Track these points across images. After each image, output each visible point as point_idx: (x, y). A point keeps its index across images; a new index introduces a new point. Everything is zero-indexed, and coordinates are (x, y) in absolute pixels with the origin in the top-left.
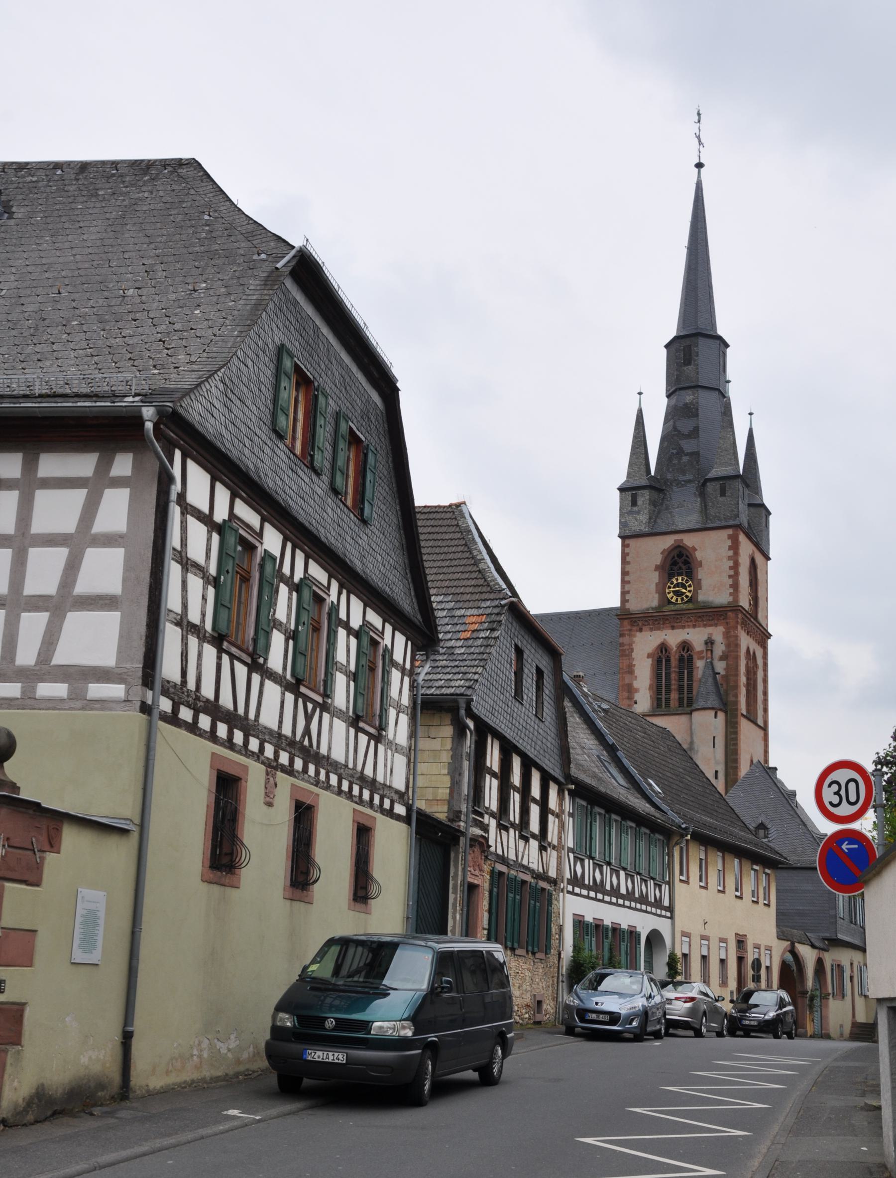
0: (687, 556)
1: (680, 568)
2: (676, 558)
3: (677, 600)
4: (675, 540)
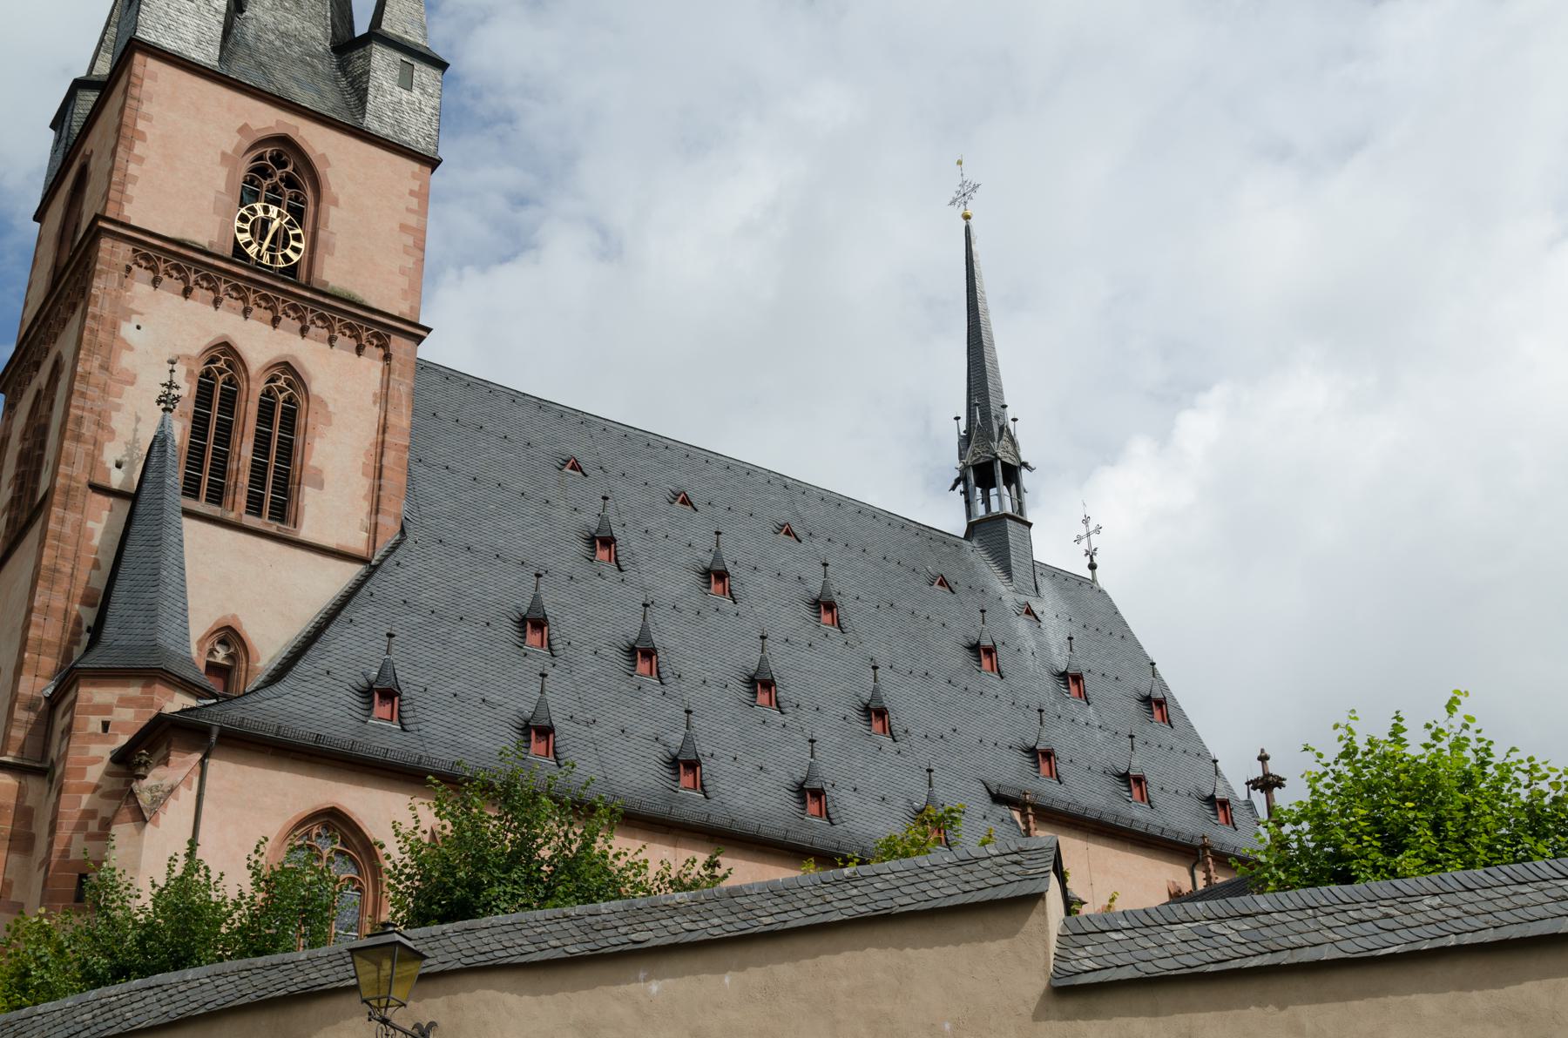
4: (277, 121)
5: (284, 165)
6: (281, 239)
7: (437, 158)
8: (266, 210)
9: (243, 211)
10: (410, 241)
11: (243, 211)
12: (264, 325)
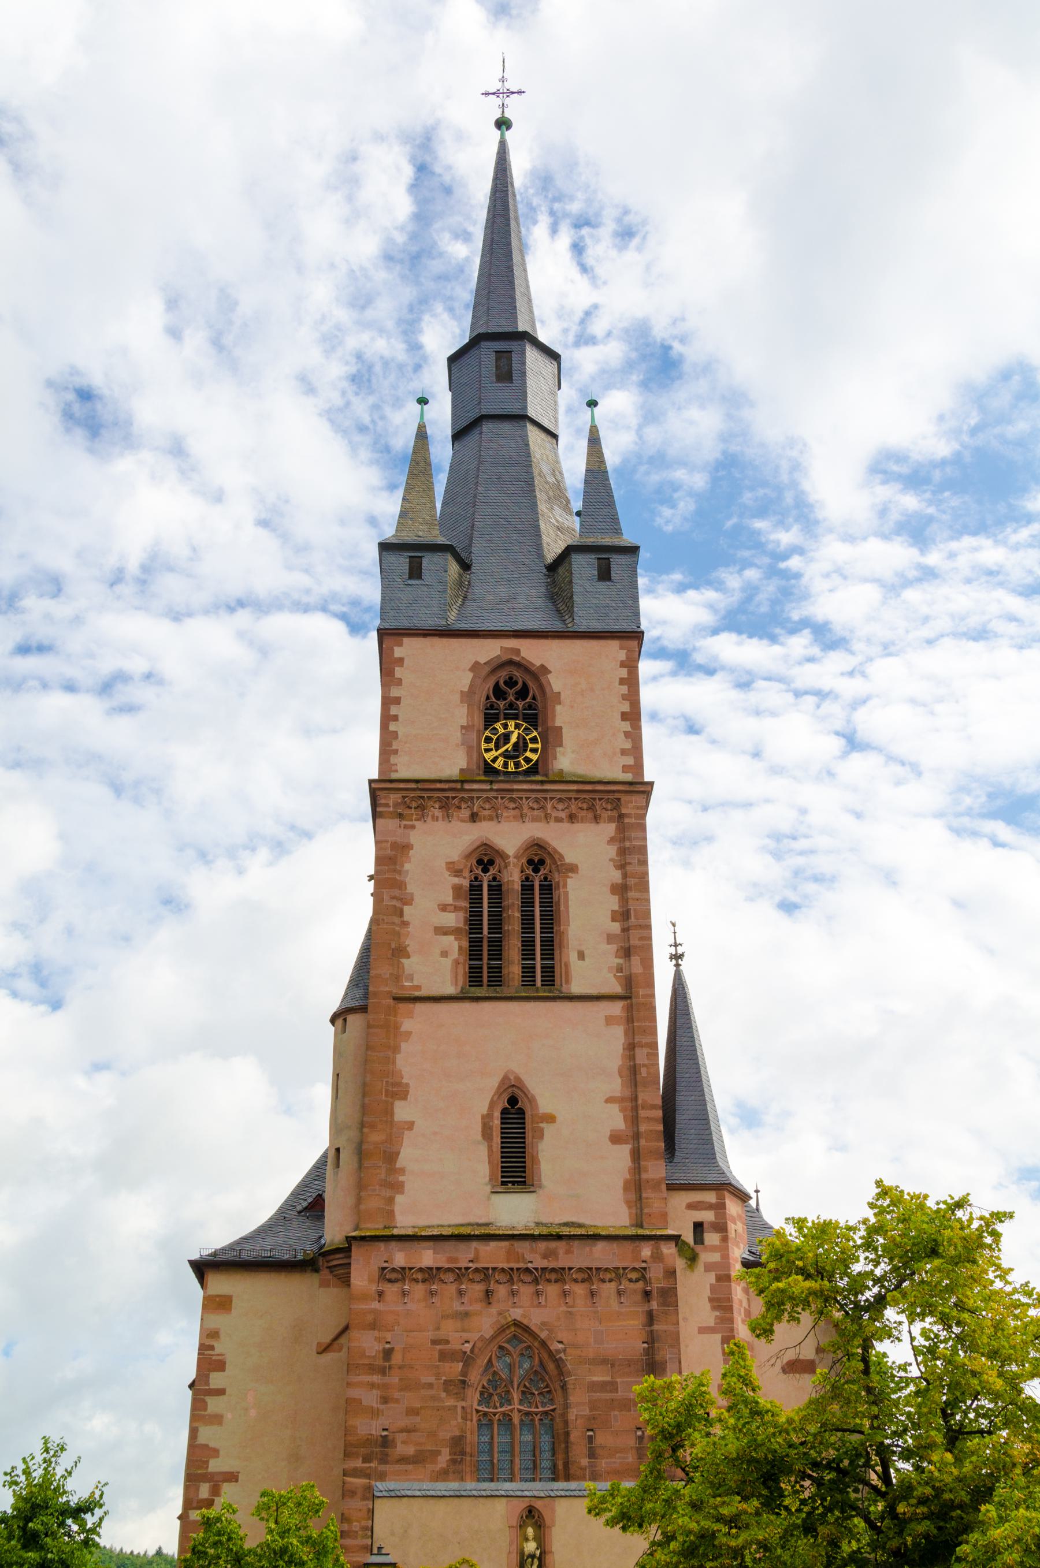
5: (516, 683)
6: (520, 747)
7: (639, 630)
8: (505, 726)
9: (487, 733)
11: (487, 733)
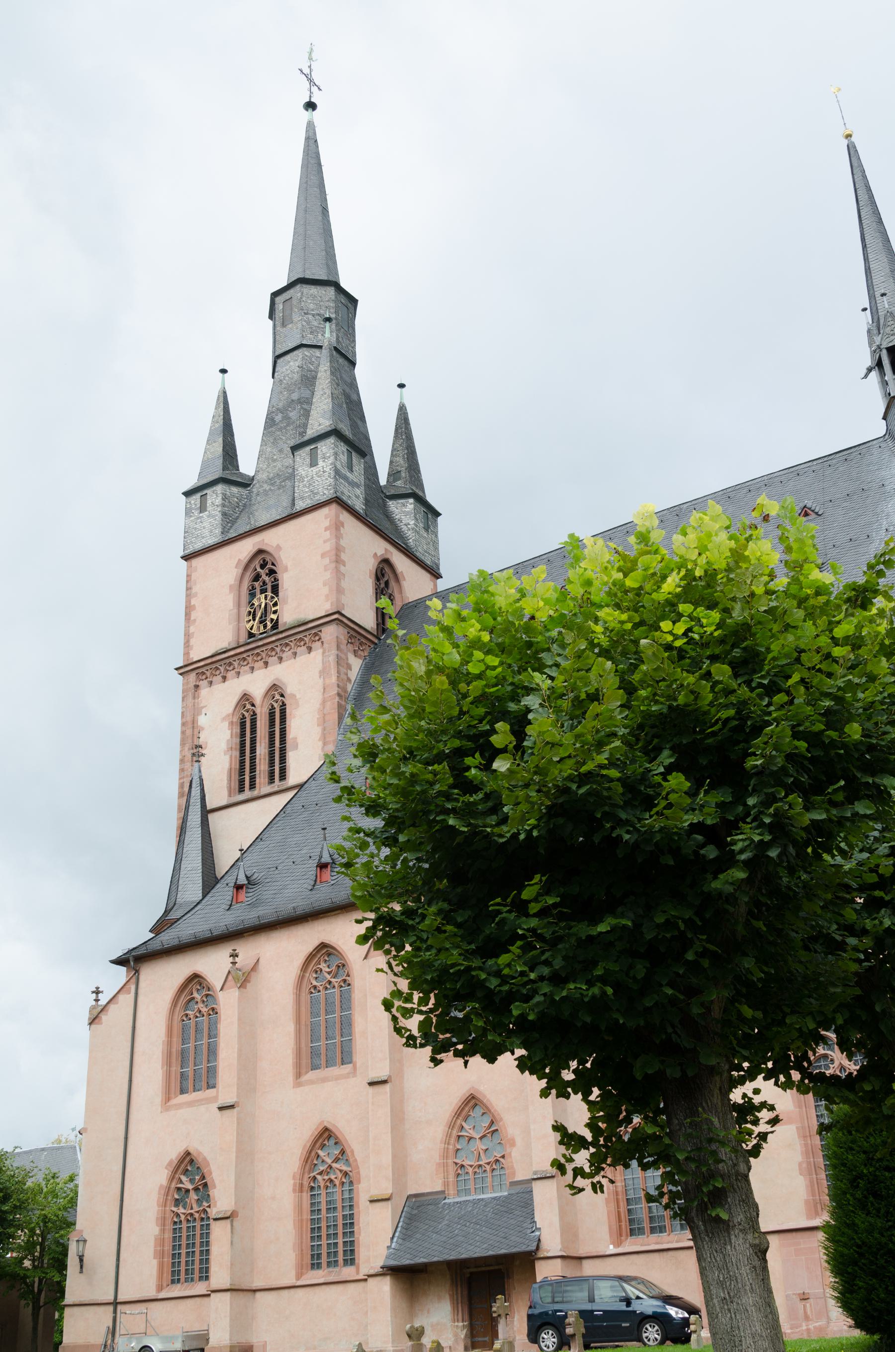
0: (273, 564)
1: (264, 583)
2: (259, 570)
3: (259, 628)
10: (327, 561)
12: (261, 671)
